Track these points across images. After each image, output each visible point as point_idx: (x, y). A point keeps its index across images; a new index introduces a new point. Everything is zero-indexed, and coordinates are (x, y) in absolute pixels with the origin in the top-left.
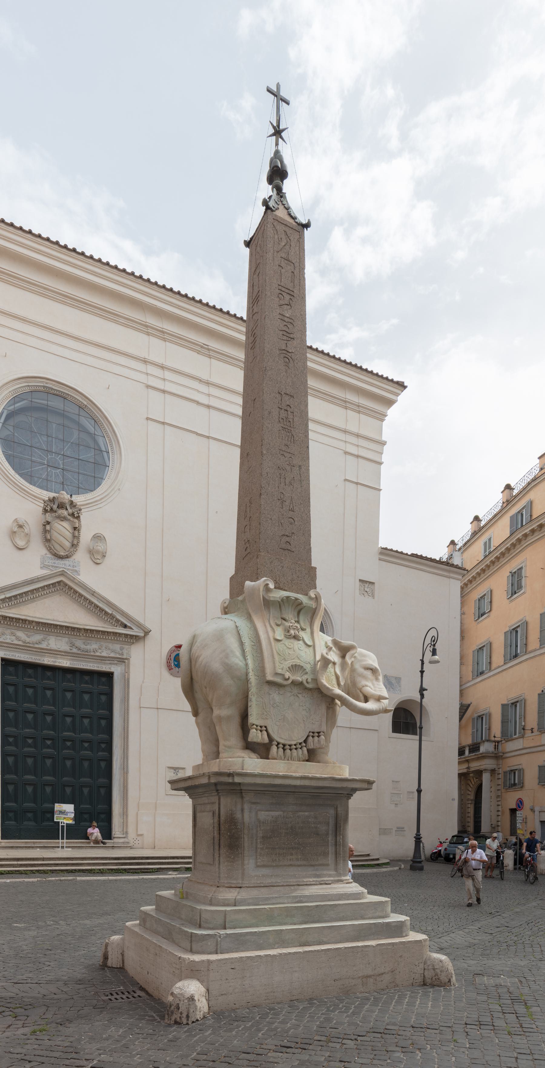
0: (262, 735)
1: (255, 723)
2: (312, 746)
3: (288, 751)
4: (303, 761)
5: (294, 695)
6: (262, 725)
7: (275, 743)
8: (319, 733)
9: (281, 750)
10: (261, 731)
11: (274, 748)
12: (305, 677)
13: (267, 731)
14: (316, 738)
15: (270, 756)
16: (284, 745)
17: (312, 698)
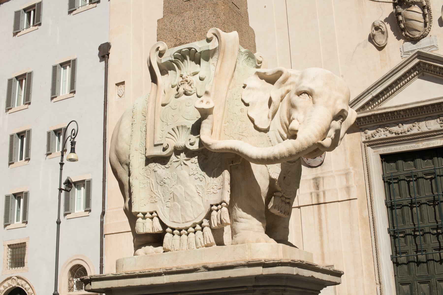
6: (151, 211)
7: (168, 230)
8: (221, 204)
10: (152, 218)
11: (168, 236)
13: (158, 217)
16: (180, 230)
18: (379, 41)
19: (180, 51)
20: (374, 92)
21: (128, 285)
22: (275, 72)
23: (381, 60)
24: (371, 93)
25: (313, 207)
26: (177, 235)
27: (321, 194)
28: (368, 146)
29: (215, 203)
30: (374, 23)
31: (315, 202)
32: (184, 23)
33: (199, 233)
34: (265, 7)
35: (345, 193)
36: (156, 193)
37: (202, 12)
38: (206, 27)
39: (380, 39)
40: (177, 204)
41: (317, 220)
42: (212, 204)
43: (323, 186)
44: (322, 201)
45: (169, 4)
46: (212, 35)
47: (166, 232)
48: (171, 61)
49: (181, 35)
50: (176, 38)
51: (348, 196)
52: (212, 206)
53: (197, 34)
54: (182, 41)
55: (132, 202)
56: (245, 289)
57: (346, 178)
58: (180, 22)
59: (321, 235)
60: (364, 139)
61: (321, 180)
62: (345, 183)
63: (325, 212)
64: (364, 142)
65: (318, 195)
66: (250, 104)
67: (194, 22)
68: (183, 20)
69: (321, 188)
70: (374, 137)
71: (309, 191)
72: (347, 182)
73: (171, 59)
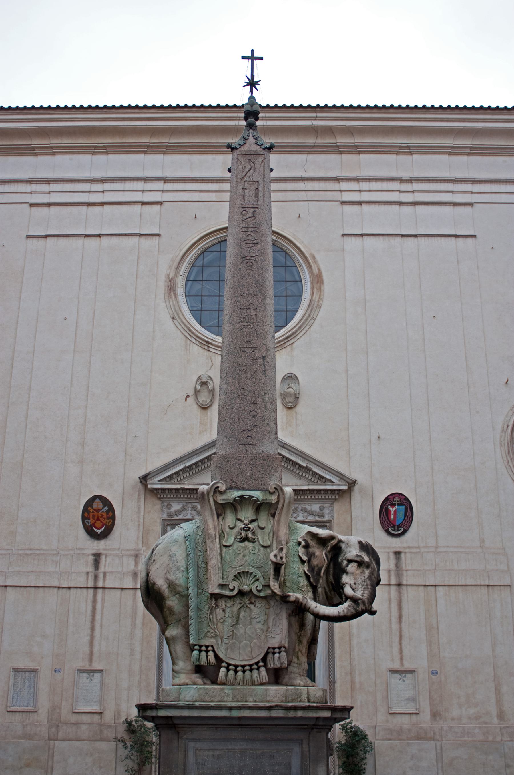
0: (207, 656)
1: (195, 643)
2: (272, 665)
3: (240, 674)
4: (262, 684)
5: (243, 606)
6: (207, 644)
9: (231, 673)
11: (223, 670)
12: (257, 583)
13: (214, 651)
14: (277, 655)
15: (218, 682)
16: (236, 666)
17: (268, 607)
18: (202, 399)
19: (241, 497)
20: (187, 462)
21: (199, 715)
22: (326, 535)
23: (201, 423)
24: (185, 461)
25: (87, 592)
26: (233, 670)
27: (101, 576)
28: (168, 525)
29: (273, 646)
30: (200, 376)
31: (91, 584)
32: (240, 467)
33: (255, 672)
34: (65, 319)
35: (131, 579)
36: (214, 629)
37: (260, 461)
38: (264, 477)
39: (204, 398)
40: (237, 643)
41: (90, 608)
42: (270, 646)
43: (105, 566)
44: (100, 584)
45: (223, 442)
46: (274, 490)
47: (221, 667)
48: (232, 504)
49: (237, 478)
50: (232, 480)
51: (134, 583)
52: (269, 648)
53: (254, 482)
54: (239, 484)
55: (190, 634)
56: (306, 727)
57: (135, 561)
58: (237, 465)
59: (93, 629)
60: (165, 516)
61: (103, 558)
62: (132, 567)
63: (102, 600)
64: (164, 520)
65: (96, 577)
66: (307, 561)
67: (252, 469)
68: (241, 464)
69: (102, 569)
70: (177, 516)
71: (85, 569)
72: (135, 566)
73: (232, 502)
